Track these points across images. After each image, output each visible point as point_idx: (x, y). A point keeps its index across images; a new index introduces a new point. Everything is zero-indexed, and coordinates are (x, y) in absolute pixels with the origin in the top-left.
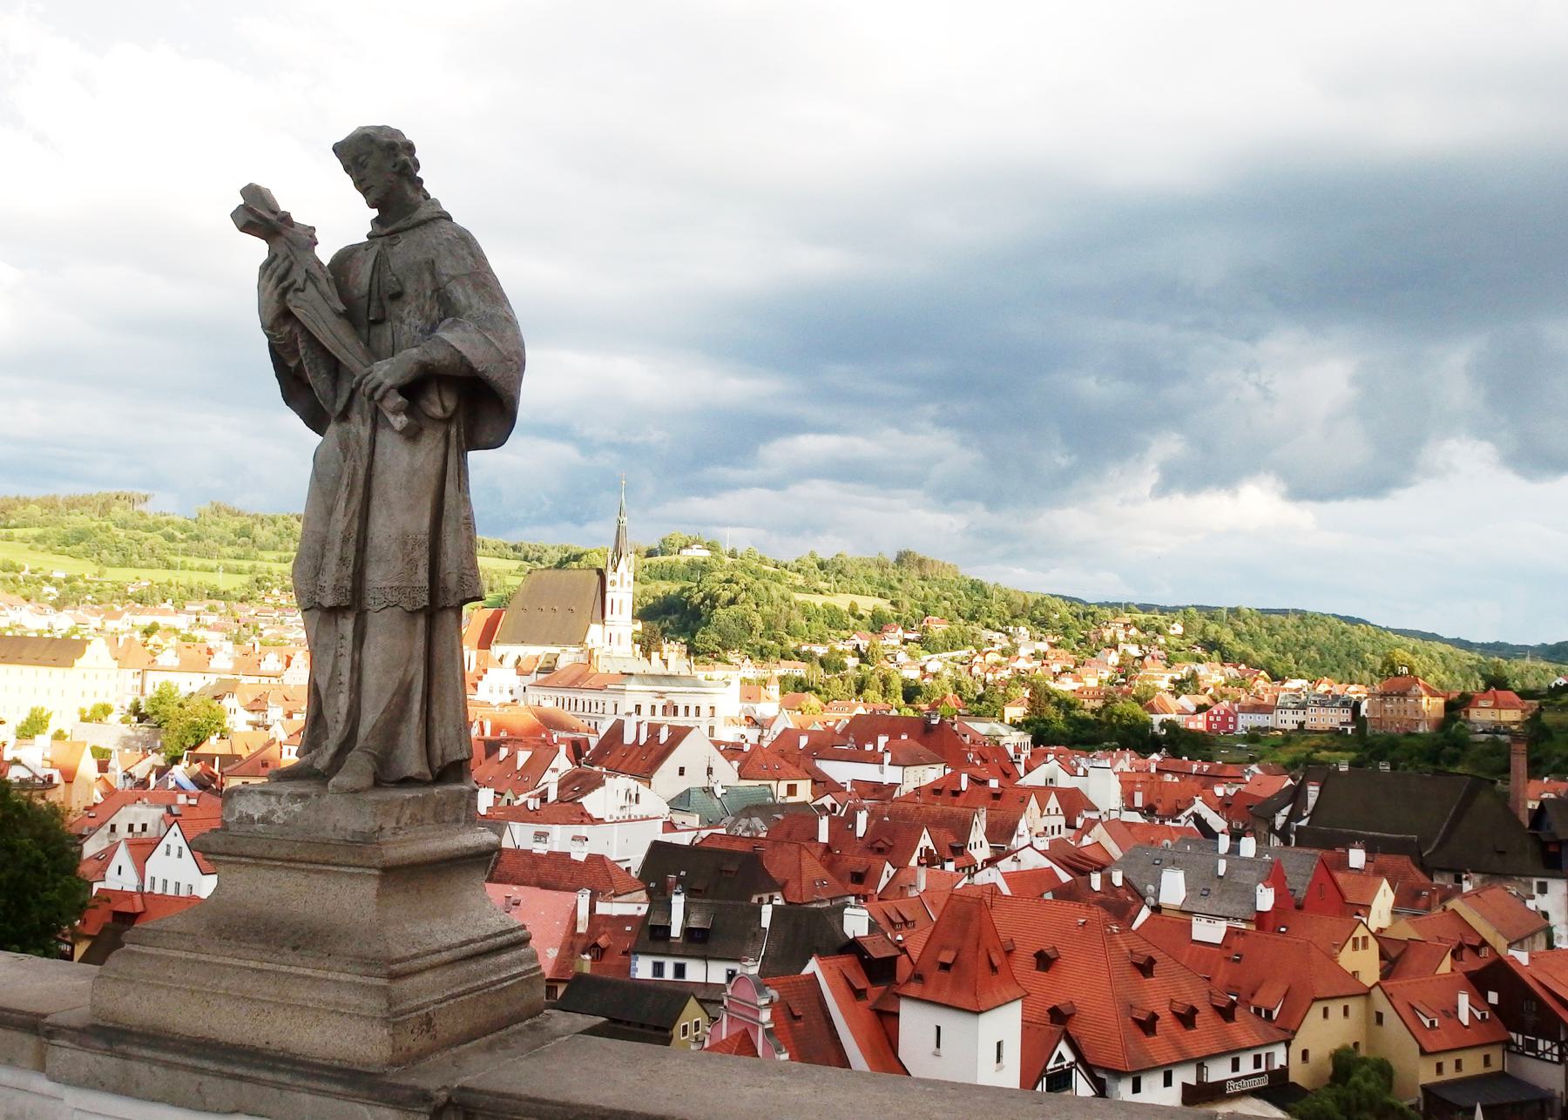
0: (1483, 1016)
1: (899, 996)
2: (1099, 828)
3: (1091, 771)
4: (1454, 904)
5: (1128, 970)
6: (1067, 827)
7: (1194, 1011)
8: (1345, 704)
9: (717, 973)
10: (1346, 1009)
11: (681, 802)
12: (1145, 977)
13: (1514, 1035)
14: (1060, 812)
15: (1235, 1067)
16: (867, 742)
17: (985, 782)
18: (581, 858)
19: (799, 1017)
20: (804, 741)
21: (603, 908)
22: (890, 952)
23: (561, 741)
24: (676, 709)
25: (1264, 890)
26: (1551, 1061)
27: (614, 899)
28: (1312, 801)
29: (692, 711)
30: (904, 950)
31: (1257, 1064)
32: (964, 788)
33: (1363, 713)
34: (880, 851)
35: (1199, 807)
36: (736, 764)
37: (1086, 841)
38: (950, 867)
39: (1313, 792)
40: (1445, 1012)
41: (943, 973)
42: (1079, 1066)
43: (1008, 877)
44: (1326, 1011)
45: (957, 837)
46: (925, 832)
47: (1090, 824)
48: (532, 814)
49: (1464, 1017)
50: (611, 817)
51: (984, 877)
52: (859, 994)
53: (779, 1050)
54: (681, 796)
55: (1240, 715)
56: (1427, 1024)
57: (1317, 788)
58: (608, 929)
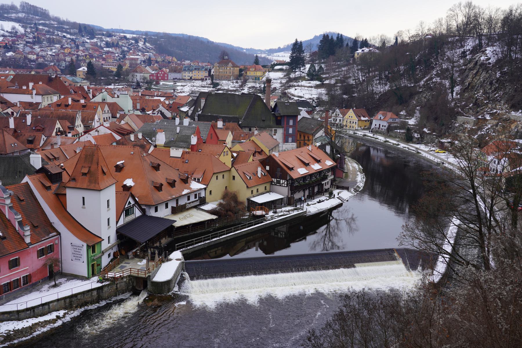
0: (265, 174)
1: (65, 187)
2: (127, 118)
3: (120, 96)
4: (253, 138)
6: (112, 117)
7: (175, 181)
8: (206, 70)
10: (223, 175)
12: (157, 171)
13: (273, 179)
14: (109, 112)
15: (189, 199)
16: (23, 85)
17: (78, 101)
19: (23, 200)
22: (61, 170)
25: (194, 137)
26: (284, 186)
28: (202, 105)
30: (64, 169)
31: (196, 197)
32: (70, 104)
33: (212, 73)
34: (39, 130)
35: (161, 108)
37: (123, 122)
38: (70, 135)
39: (203, 102)
40: (253, 174)
41: (84, 177)
42: (136, 205)
43: (95, 138)
44: (217, 176)
45: (71, 123)
46: (58, 122)
47: (123, 117)
49: (259, 175)
51: (85, 138)
52: (48, 188)
53: (16, 214)
55: (169, 74)
57: (204, 100)
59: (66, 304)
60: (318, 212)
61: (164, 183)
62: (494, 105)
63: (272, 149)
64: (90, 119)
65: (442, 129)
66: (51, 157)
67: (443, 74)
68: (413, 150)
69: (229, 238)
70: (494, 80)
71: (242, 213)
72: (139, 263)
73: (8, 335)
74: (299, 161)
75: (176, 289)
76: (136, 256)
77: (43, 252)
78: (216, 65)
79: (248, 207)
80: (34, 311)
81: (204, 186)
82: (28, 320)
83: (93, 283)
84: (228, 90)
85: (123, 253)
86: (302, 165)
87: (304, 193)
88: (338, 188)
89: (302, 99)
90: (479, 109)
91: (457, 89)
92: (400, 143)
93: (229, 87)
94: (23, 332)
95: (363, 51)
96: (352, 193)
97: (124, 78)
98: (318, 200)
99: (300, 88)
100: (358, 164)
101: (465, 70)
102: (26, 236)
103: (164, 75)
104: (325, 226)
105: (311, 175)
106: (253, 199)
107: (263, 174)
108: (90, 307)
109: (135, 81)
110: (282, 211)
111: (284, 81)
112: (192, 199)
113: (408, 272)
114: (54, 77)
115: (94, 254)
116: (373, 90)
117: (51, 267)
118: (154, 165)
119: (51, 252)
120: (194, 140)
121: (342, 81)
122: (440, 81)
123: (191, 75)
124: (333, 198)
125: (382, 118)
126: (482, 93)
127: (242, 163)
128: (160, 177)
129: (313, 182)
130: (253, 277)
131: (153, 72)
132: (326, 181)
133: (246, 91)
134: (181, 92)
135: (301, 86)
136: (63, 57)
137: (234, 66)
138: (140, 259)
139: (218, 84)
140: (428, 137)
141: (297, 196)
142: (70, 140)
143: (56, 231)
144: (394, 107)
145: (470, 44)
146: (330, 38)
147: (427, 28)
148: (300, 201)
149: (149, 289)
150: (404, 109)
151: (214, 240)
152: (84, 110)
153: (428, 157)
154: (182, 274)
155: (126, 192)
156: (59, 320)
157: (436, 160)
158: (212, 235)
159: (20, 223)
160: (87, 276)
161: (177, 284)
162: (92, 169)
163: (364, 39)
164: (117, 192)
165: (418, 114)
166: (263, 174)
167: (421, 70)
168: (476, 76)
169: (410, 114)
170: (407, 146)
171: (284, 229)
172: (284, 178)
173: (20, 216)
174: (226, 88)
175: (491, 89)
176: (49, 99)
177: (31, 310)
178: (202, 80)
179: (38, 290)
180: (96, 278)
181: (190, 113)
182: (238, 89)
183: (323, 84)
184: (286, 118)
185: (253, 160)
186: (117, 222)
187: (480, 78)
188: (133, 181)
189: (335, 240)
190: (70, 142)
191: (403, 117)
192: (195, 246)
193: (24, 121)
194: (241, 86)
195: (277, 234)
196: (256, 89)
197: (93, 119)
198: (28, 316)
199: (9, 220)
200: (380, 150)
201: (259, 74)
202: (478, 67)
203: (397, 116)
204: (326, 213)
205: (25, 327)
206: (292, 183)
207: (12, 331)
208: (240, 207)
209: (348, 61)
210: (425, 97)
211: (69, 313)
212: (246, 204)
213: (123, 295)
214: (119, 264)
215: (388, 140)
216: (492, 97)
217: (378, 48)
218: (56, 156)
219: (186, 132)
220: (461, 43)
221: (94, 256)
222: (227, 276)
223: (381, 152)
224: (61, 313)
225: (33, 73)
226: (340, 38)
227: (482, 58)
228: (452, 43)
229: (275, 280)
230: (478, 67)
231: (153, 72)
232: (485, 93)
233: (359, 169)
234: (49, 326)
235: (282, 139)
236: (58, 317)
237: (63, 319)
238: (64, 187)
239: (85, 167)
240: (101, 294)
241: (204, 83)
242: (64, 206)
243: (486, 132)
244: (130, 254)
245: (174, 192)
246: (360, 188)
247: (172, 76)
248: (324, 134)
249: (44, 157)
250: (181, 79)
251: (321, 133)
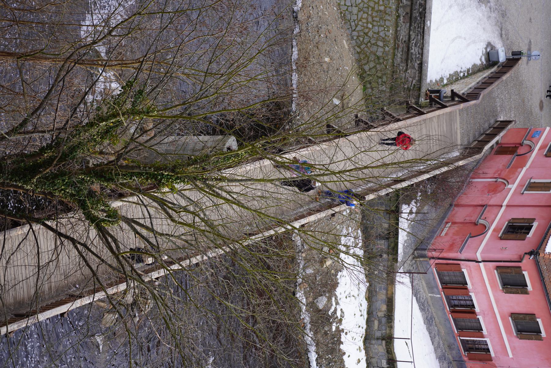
94: (331, 354)
198: (373, 361)
205: (345, 358)
207: (337, 328)
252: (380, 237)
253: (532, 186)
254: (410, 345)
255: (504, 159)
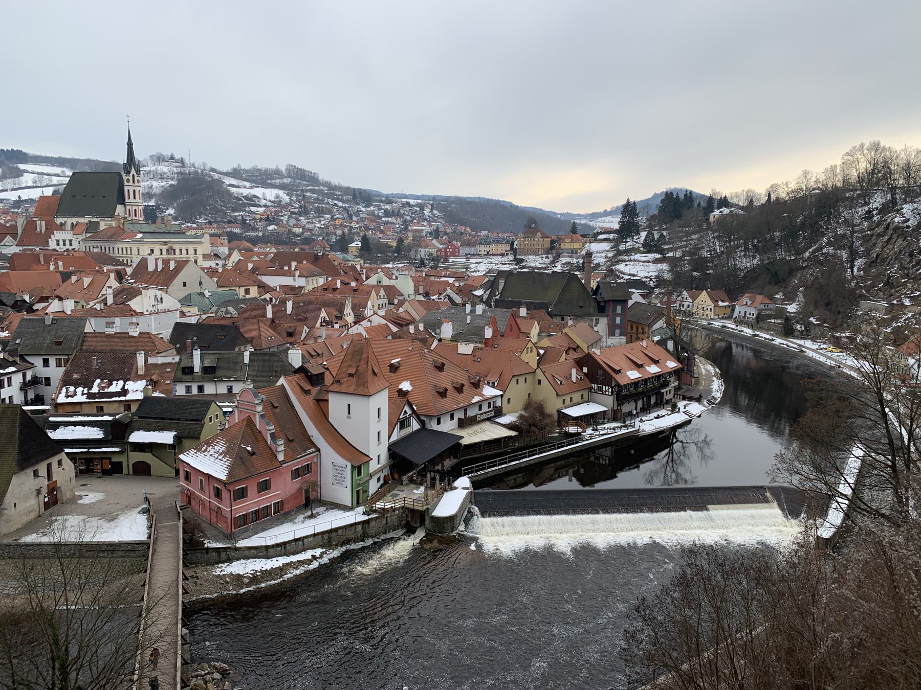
0: (581, 378)
2: (406, 304)
3: (399, 277)
4: (566, 330)
5: (432, 369)
6: (389, 304)
7: (463, 385)
8: (507, 242)
9: (222, 389)
10: (526, 378)
11: (186, 301)
12: (440, 372)
13: (593, 385)
14: (386, 297)
15: (480, 409)
16: (285, 265)
17: (349, 284)
18: (136, 334)
19: (277, 407)
20: (250, 266)
21: (151, 360)
22: (323, 370)
23: (109, 271)
24: (174, 250)
25: (489, 329)
27: (158, 355)
28: (501, 287)
29: (184, 252)
30: (327, 369)
31: (489, 407)
33: (515, 246)
34: (300, 320)
35: (449, 291)
36: (215, 279)
37: (401, 310)
38: (337, 326)
39: (502, 283)
41: (350, 378)
43: (367, 329)
44: (517, 380)
45: (338, 311)
46: (323, 309)
47: (401, 303)
48: (99, 312)
49: (574, 379)
50: (147, 311)
51: (355, 330)
52: (307, 392)
53: (268, 424)
54: (186, 297)
56: (559, 383)
58: (157, 372)
59: (325, 541)
60: (655, 431)
61: (450, 387)
62: (917, 285)
63: (592, 345)
64: (361, 306)
65: (837, 319)
66: (314, 353)
67: (837, 243)
68: (795, 348)
69: (532, 462)
70: (915, 250)
71: (550, 429)
72: (415, 491)
73: (254, 577)
74: (629, 360)
75: (462, 528)
76: (412, 481)
77: (298, 472)
78: (521, 235)
79: (559, 422)
80: (285, 547)
81: (501, 393)
82: (277, 558)
83: (357, 516)
84: (536, 268)
85: (396, 476)
86: (633, 366)
87: (636, 404)
88: (684, 398)
89: (636, 278)
90: (893, 291)
91: (859, 262)
92: (774, 338)
93: (537, 264)
95: (721, 212)
96: (705, 406)
97: (405, 255)
98: (655, 414)
99: (632, 263)
100: (713, 367)
101: (872, 236)
102: (279, 452)
103: (454, 250)
104: (666, 451)
105: (645, 381)
106: (564, 411)
107: (579, 378)
108: (354, 546)
109: (419, 257)
110: (604, 429)
111: (610, 255)
112: (485, 408)
113: (785, 519)
114: (321, 254)
115: (360, 477)
116: (735, 265)
117: (307, 491)
118: (437, 365)
119: (308, 473)
120: (489, 333)
121: (691, 254)
122: (834, 251)
123: (488, 249)
124: (677, 412)
125: (749, 303)
126: (898, 268)
127: (551, 363)
128: (445, 380)
129: (648, 390)
130: (564, 517)
131: (441, 247)
132: (667, 389)
133: (558, 269)
134: (475, 271)
135: (634, 261)
136: (333, 230)
137: (544, 236)
138: (418, 486)
139: (522, 260)
140: (817, 329)
141: (626, 408)
142: (337, 332)
143: (316, 447)
144: (766, 288)
145: (877, 201)
146: (675, 196)
147: (814, 179)
148: (630, 414)
149: (427, 526)
150: (781, 291)
151: (512, 463)
152: (355, 295)
153: (818, 359)
154: (469, 508)
155: (401, 399)
156: (315, 561)
157: (828, 362)
158: (509, 457)
159: (272, 435)
160: (350, 505)
161: (464, 521)
162: (360, 369)
163: (723, 196)
164: (390, 399)
165: (801, 297)
166: (579, 378)
167: (805, 236)
168: (887, 245)
169: (790, 298)
170: (785, 342)
171: (608, 452)
172: (609, 385)
173: (272, 427)
174: (533, 265)
175: (910, 262)
176: (315, 282)
177: (281, 547)
178: (502, 255)
179: (291, 521)
180: (361, 509)
181: (485, 297)
182: (549, 266)
183: (664, 257)
184: (611, 303)
185: (566, 359)
186: (389, 437)
187: (894, 247)
188: (410, 384)
189: (681, 470)
190: (336, 334)
191: (779, 302)
192: (488, 471)
193: (283, 309)
194: (553, 262)
195: (598, 459)
196: (572, 266)
197: (365, 307)
199: (260, 432)
200: (747, 347)
201: (576, 245)
202: (890, 232)
203: (771, 300)
204: (668, 433)
205: (274, 567)
206: (619, 391)
208: (548, 421)
209: (700, 226)
210: (811, 275)
211: (328, 553)
212: (556, 418)
213: (395, 532)
214: (390, 491)
215: (757, 333)
216: (912, 274)
217: (742, 208)
218: (320, 353)
219: (480, 322)
220: (864, 200)
221: (360, 480)
222: (529, 514)
223: (747, 350)
224: (318, 552)
225: (296, 250)
226: (689, 197)
227: (896, 220)
228: (851, 199)
229: (594, 522)
230: (890, 232)
231: (441, 247)
232: (902, 268)
233: (716, 372)
234: (303, 568)
235: (605, 331)
236: (314, 557)
237: (320, 560)
238: (327, 391)
239: (352, 366)
240: (367, 530)
241: (505, 259)
242: (324, 414)
243: (905, 323)
244: (405, 478)
245: (462, 402)
246: (717, 399)
247: (464, 250)
248: (665, 326)
249: (306, 354)
250: (475, 255)
251: (661, 323)
252: (219, 556)
253: (202, 488)
254: (270, 538)
255: (192, 501)
